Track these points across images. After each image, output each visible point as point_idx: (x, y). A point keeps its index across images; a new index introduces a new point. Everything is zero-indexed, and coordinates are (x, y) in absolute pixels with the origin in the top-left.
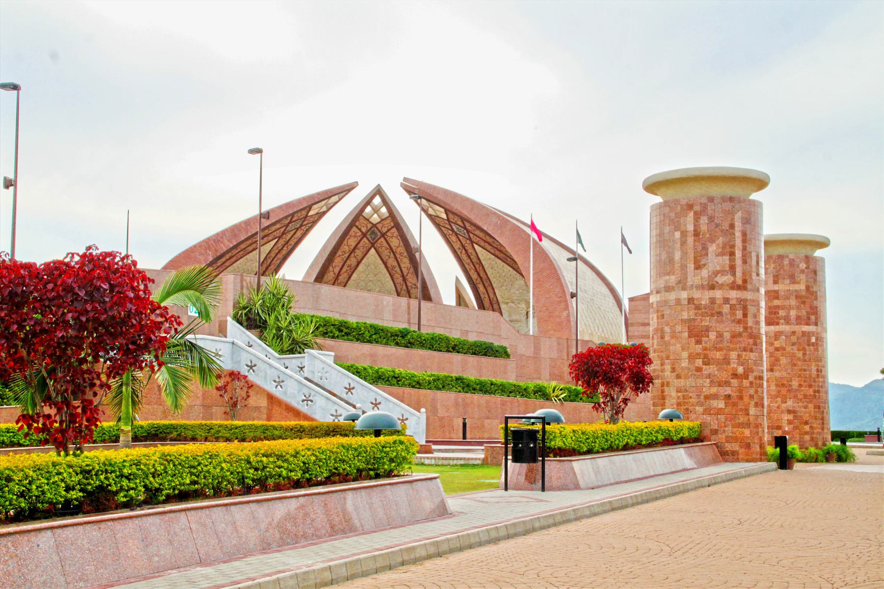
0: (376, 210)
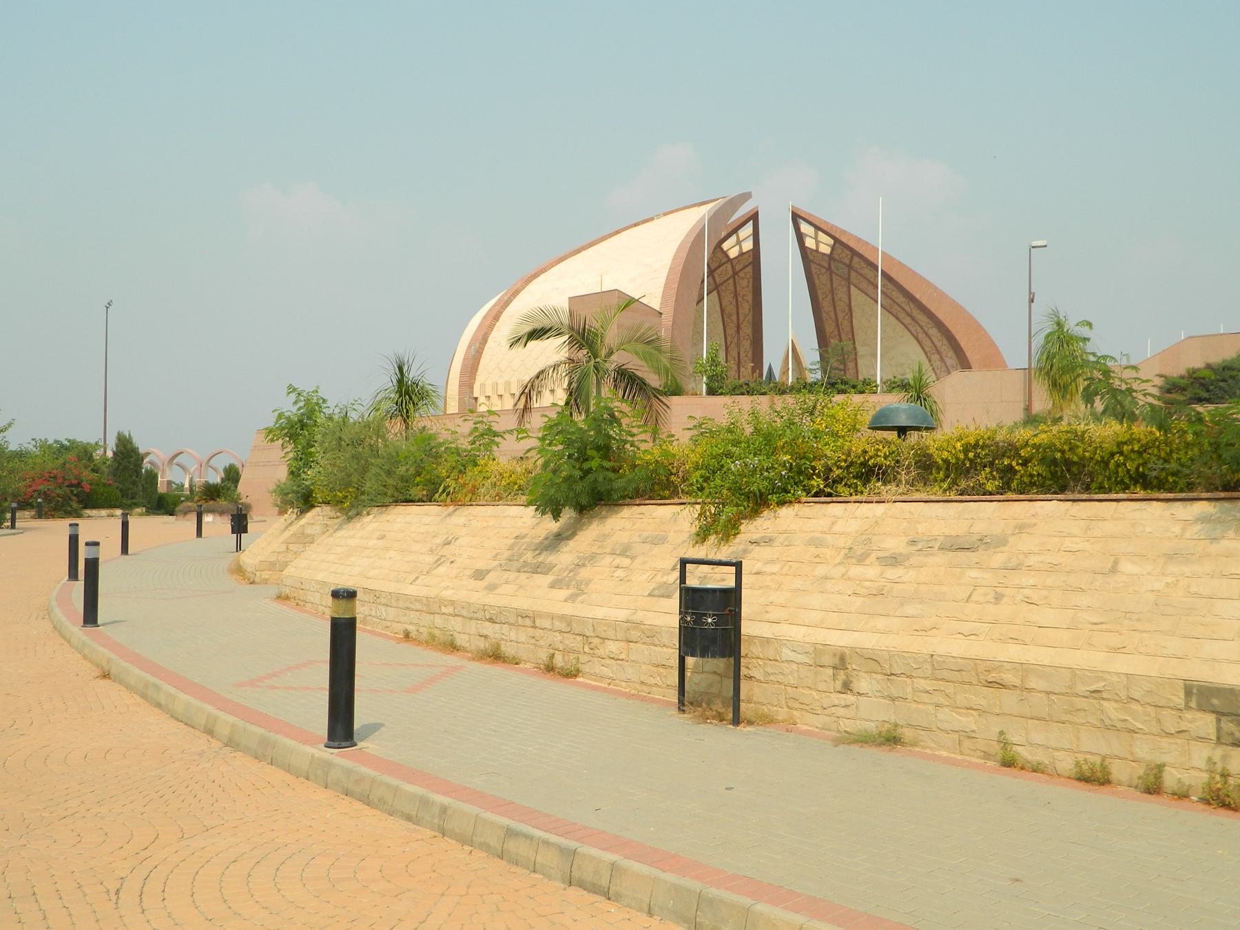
0: (739, 243)
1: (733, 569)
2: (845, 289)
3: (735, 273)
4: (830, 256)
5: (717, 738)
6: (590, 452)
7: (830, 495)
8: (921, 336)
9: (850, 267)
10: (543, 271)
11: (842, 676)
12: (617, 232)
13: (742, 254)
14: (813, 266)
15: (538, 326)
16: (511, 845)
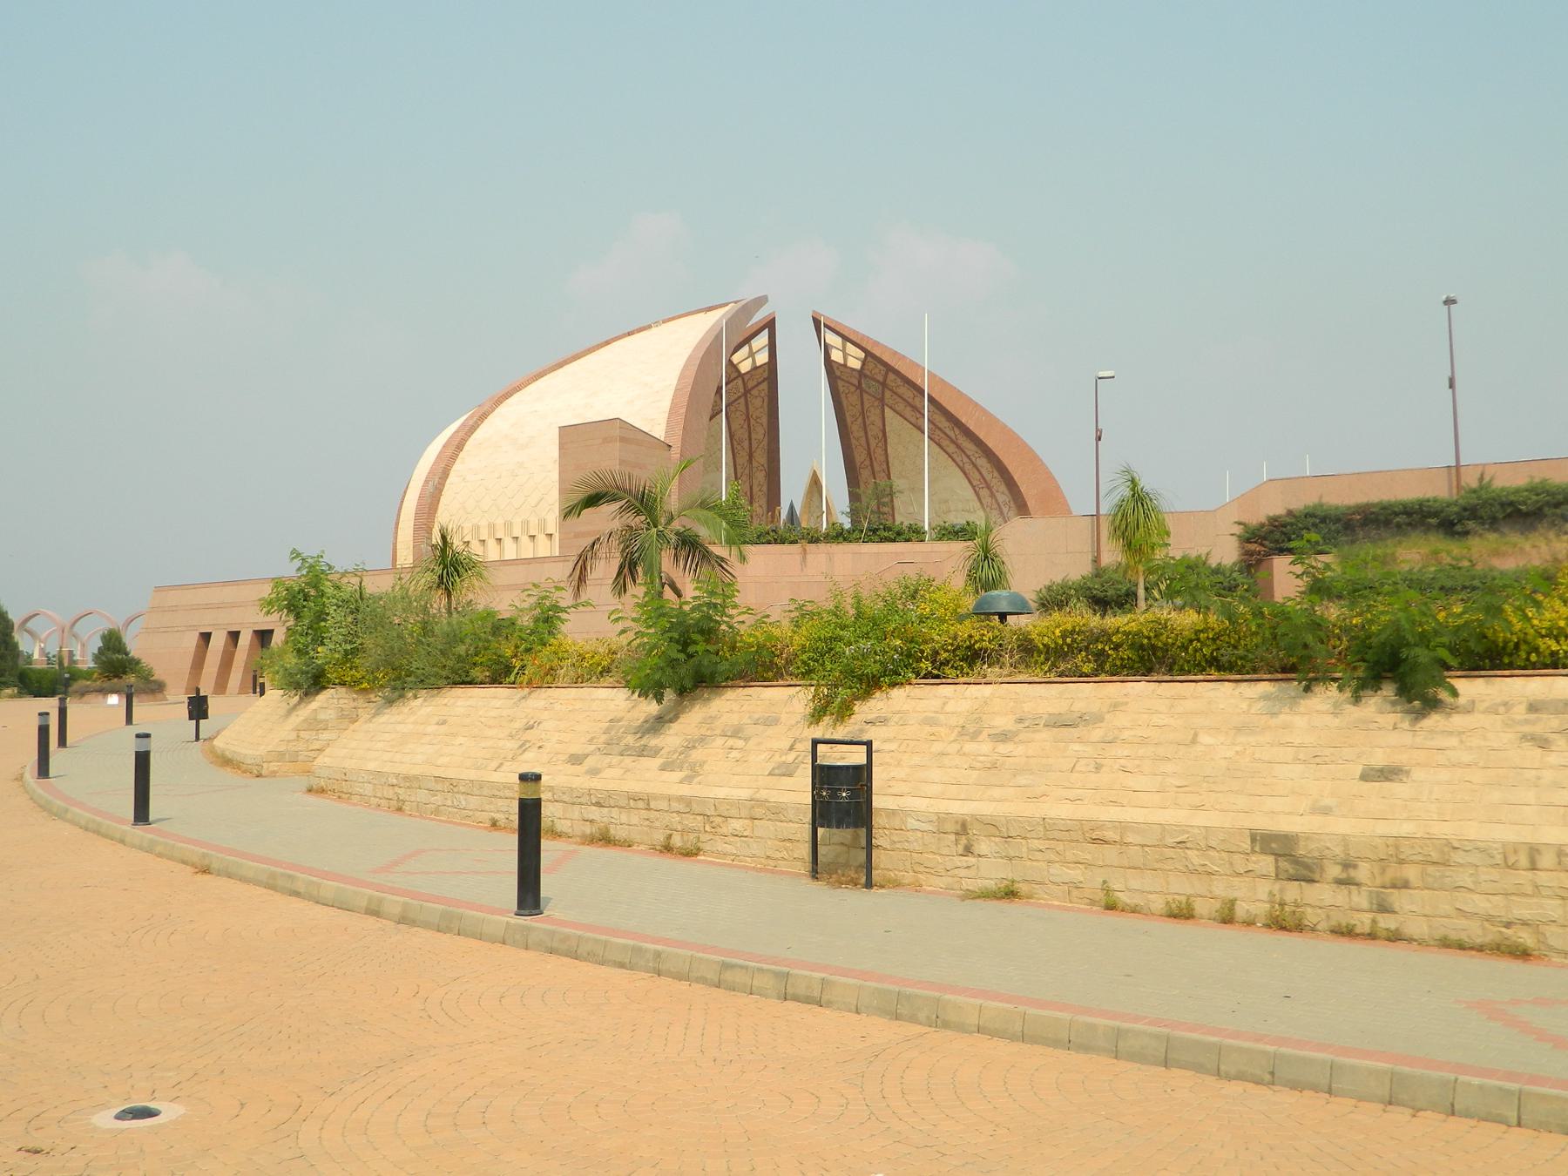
0: (752, 354)
1: (820, 747)
2: (878, 411)
3: (747, 392)
4: (861, 372)
5: (855, 899)
6: (695, 637)
7: (937, 677)
8: (968, 467)
9: (884, 385)
10: (518, 389)
11: (963, 841)
12: (607, 343)
13: (755, 368)
14: (840, 383)
15: (592, 492)
16: (728, 976)
